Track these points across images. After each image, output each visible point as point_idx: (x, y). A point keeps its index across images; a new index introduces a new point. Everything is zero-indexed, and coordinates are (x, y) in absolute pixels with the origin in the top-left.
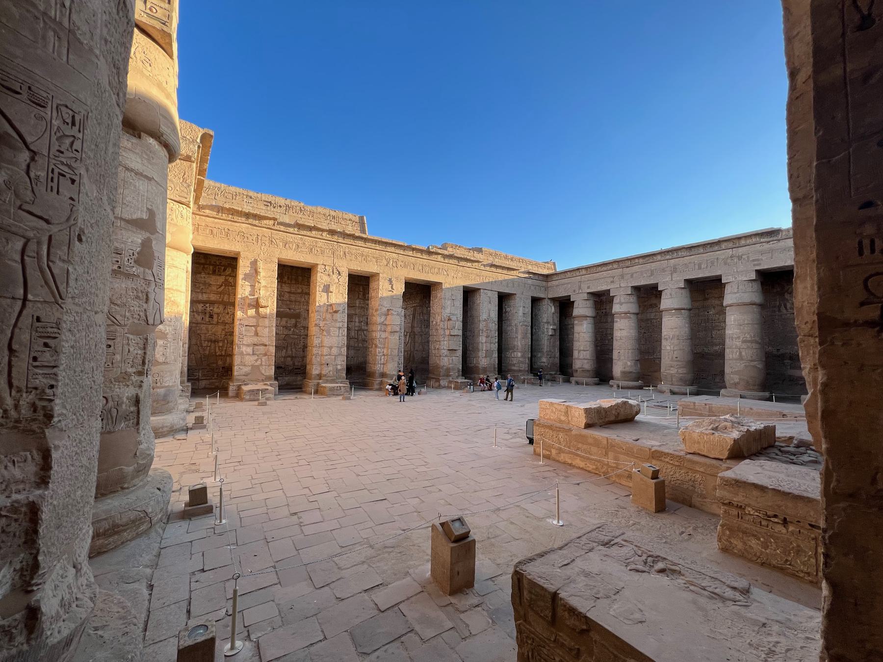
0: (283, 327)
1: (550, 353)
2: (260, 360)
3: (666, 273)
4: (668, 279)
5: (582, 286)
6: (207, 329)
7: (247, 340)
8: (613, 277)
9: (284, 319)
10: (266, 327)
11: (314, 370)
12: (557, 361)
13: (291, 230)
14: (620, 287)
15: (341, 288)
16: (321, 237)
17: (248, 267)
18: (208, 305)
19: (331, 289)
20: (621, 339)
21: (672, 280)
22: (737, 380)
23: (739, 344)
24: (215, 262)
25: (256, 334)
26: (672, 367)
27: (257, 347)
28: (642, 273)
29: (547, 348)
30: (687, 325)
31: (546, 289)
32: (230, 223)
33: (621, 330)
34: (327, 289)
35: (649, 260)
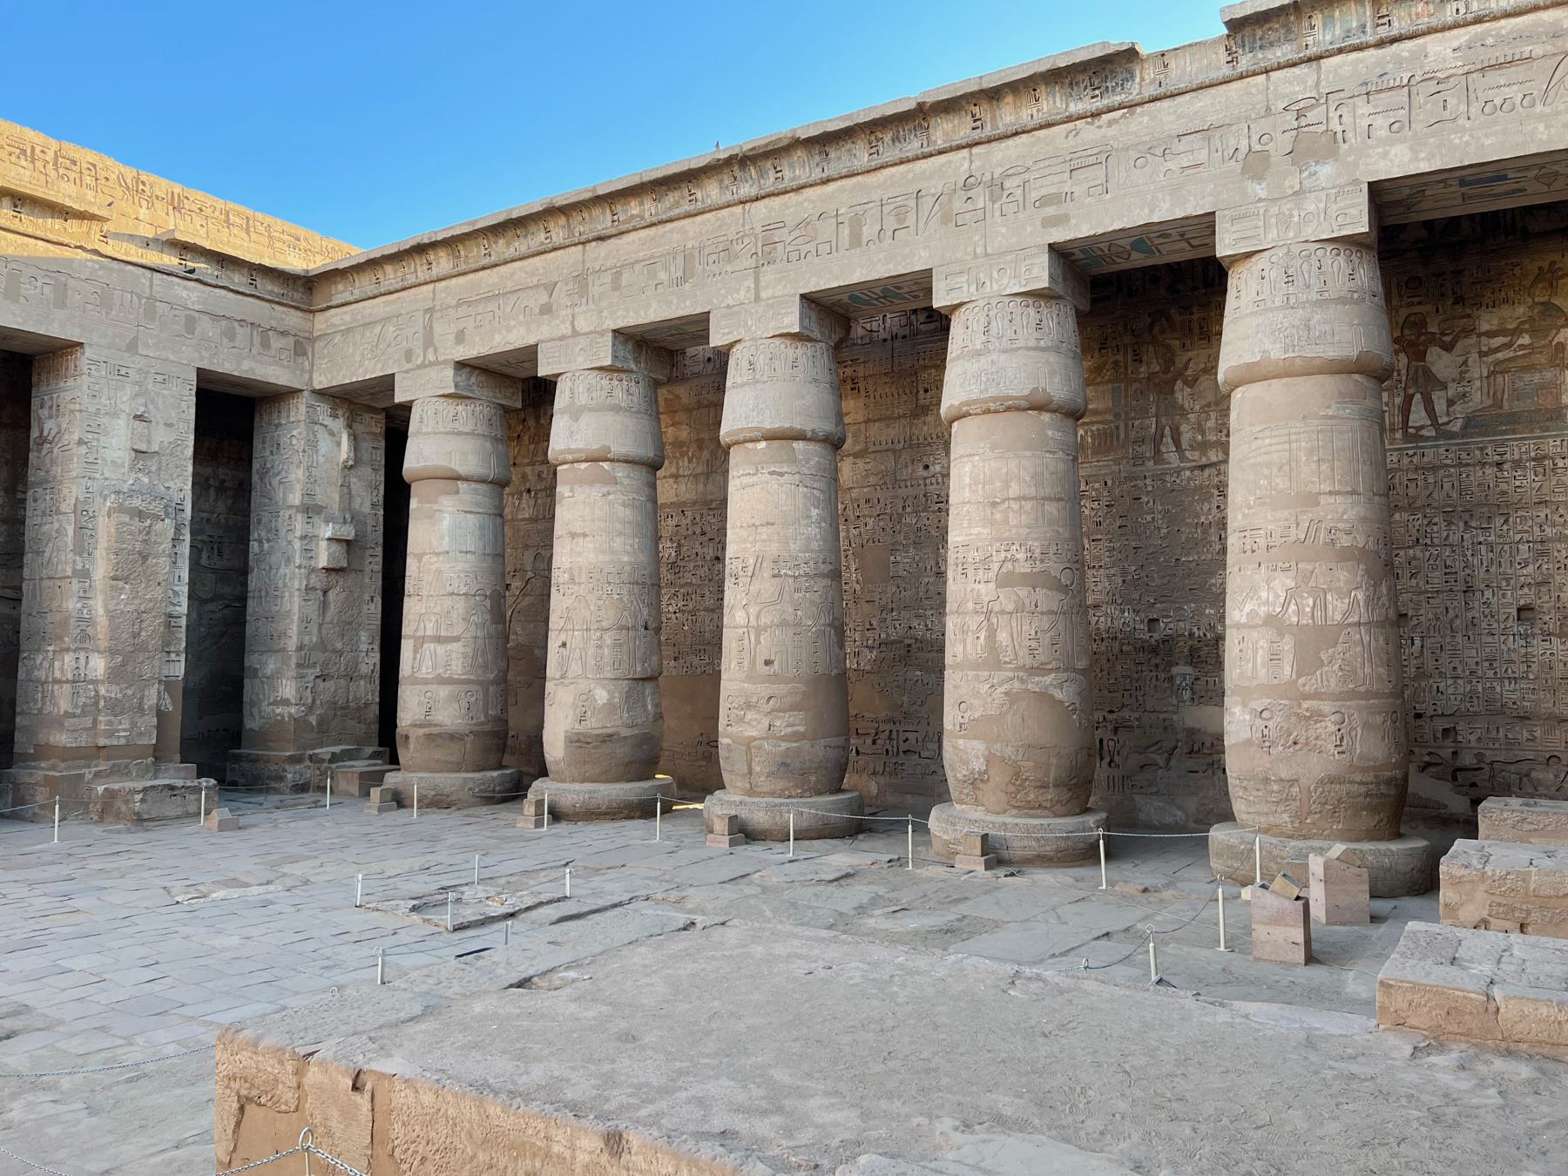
1: (319, 657)
14: (575, 333)
21: (757, 298)
22: (978, 765)
26: (749, 706)
29: (304, 631)
30: (814, 512)
31: (302, 347)
35: (677, 204)
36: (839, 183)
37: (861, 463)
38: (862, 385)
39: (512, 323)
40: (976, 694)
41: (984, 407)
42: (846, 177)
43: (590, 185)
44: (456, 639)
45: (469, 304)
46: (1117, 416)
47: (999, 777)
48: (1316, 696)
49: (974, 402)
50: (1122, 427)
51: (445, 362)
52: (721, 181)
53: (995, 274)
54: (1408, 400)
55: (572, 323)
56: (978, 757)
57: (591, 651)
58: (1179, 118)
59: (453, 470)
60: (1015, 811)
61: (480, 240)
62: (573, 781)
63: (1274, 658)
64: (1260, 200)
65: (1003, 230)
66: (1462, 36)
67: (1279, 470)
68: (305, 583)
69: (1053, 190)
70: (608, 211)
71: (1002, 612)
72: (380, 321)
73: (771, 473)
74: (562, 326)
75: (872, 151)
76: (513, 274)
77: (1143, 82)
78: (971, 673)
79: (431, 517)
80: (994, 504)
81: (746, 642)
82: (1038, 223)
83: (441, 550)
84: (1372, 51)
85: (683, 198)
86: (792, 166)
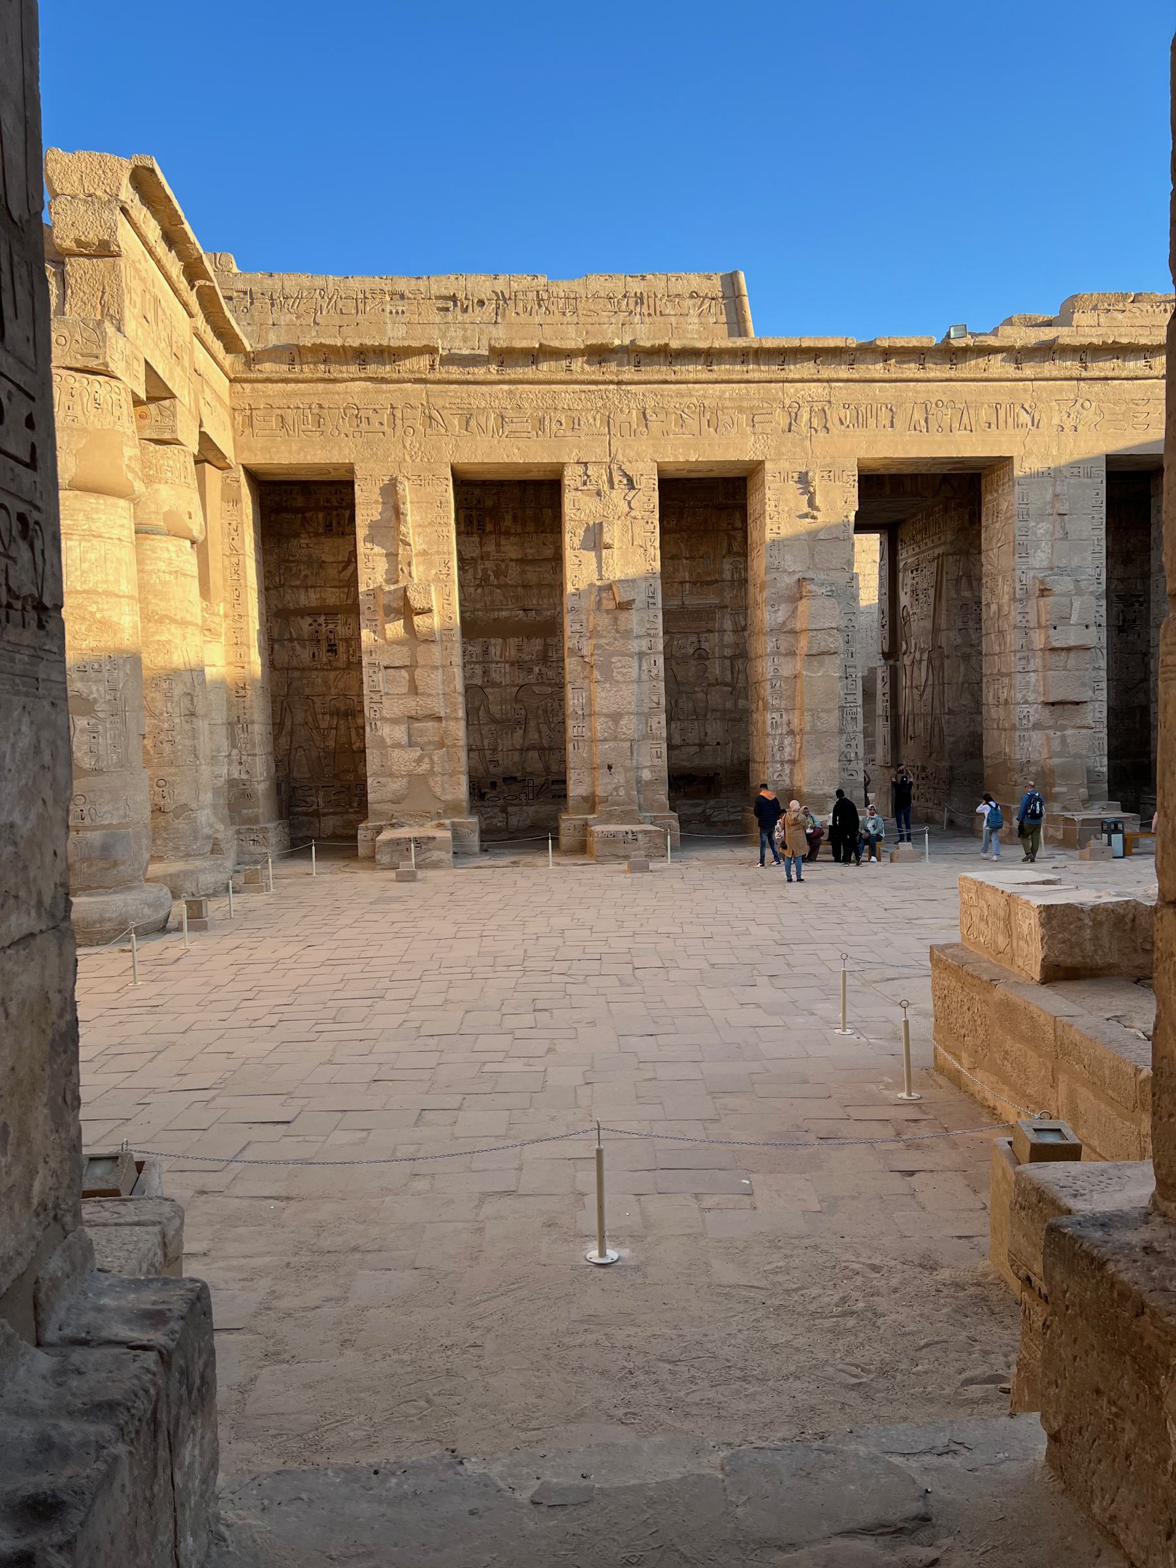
0: (512, 664)
2: (427, 760)
6: (326, 683)
7: (391, 708)
9: (513, 641)
10: (436, 668)
11: (576, 789)
13: (480, 372)
15: (637, 530)
16: (568, 377)
17: (376, 502)
18: (323, 618)
19: (607, 538)
24: (328, 501)
25: (414, 690)
27: (417, 725)
32: (321, 386)
34: (595, 540)
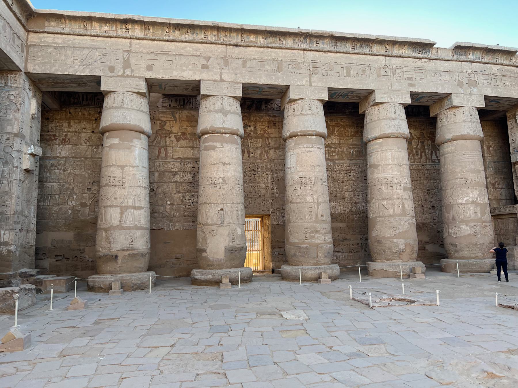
1: (22, 218)
3: (301, 71)
4: (305, 81)
5: (133, 61)
8: (208, 59)
12: (31, 238)
14: (222, 80)
20: (224, 182)
21: (311, 85)
22: (402, 247)
23: (401, 192)
26: (316, 232)
28: (262, 61)
29: (17, 204)
33: (224, 164)
35: (274, 43)
36: (341, 54)
37: (277, 152)
38: (277, 124)
39: (184, 68)
40: (400, 225)
41: (396, 135)
42: (345, 53)
43: (218, 21)
44: (142, 208)
45: (156, 54)
46: (362, 147)
47: (408, 250)
48: (485, 222)
49: (394, 133)
50: (364, 150)
51: (139, 77)
52: (294, 40)
53: (395, 96)
54: (432, 152)
55: (221, 76)
56: (402, 244)
57: (235, 212)
58: (442, 66)
59: (142, 128)
60: (411, 261)
61: (165, 28)
62: (227, 268)
63: (476, 212)
64: (462, 93)
65: (397, 84)
66: (499, 67)
67: (472, 163)
68: (19, 177)
69: (410, 76)
70: (240, 36)
71: (405, 199)
72: (88, 48)
73: (318, 148)
74: (215, 76)
75: (353, 47)
76: (185, 48)
77: (432, 54)
78: (397, 218)
79: (129, 149)
80: (400, 166)
81: (313, 208)
82: (407, 84)
83: (135, 165)
84: (482, 64)
85: (277, 41)
86: (323, 43)
